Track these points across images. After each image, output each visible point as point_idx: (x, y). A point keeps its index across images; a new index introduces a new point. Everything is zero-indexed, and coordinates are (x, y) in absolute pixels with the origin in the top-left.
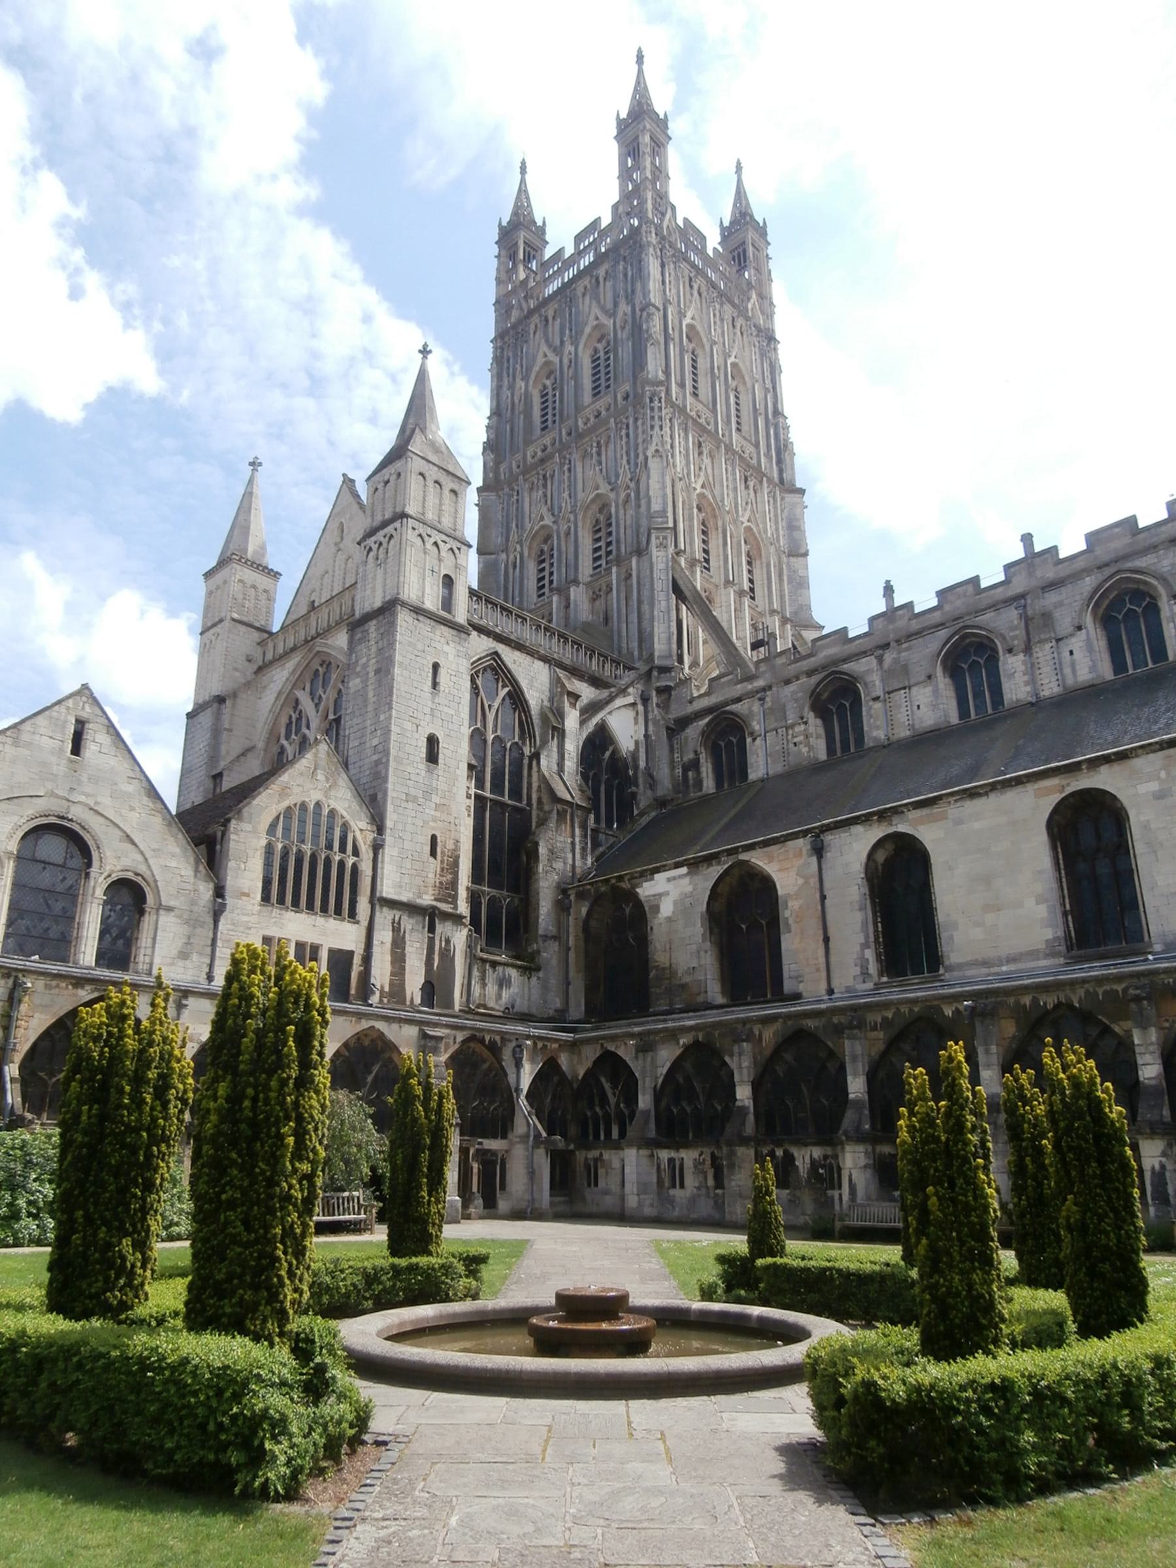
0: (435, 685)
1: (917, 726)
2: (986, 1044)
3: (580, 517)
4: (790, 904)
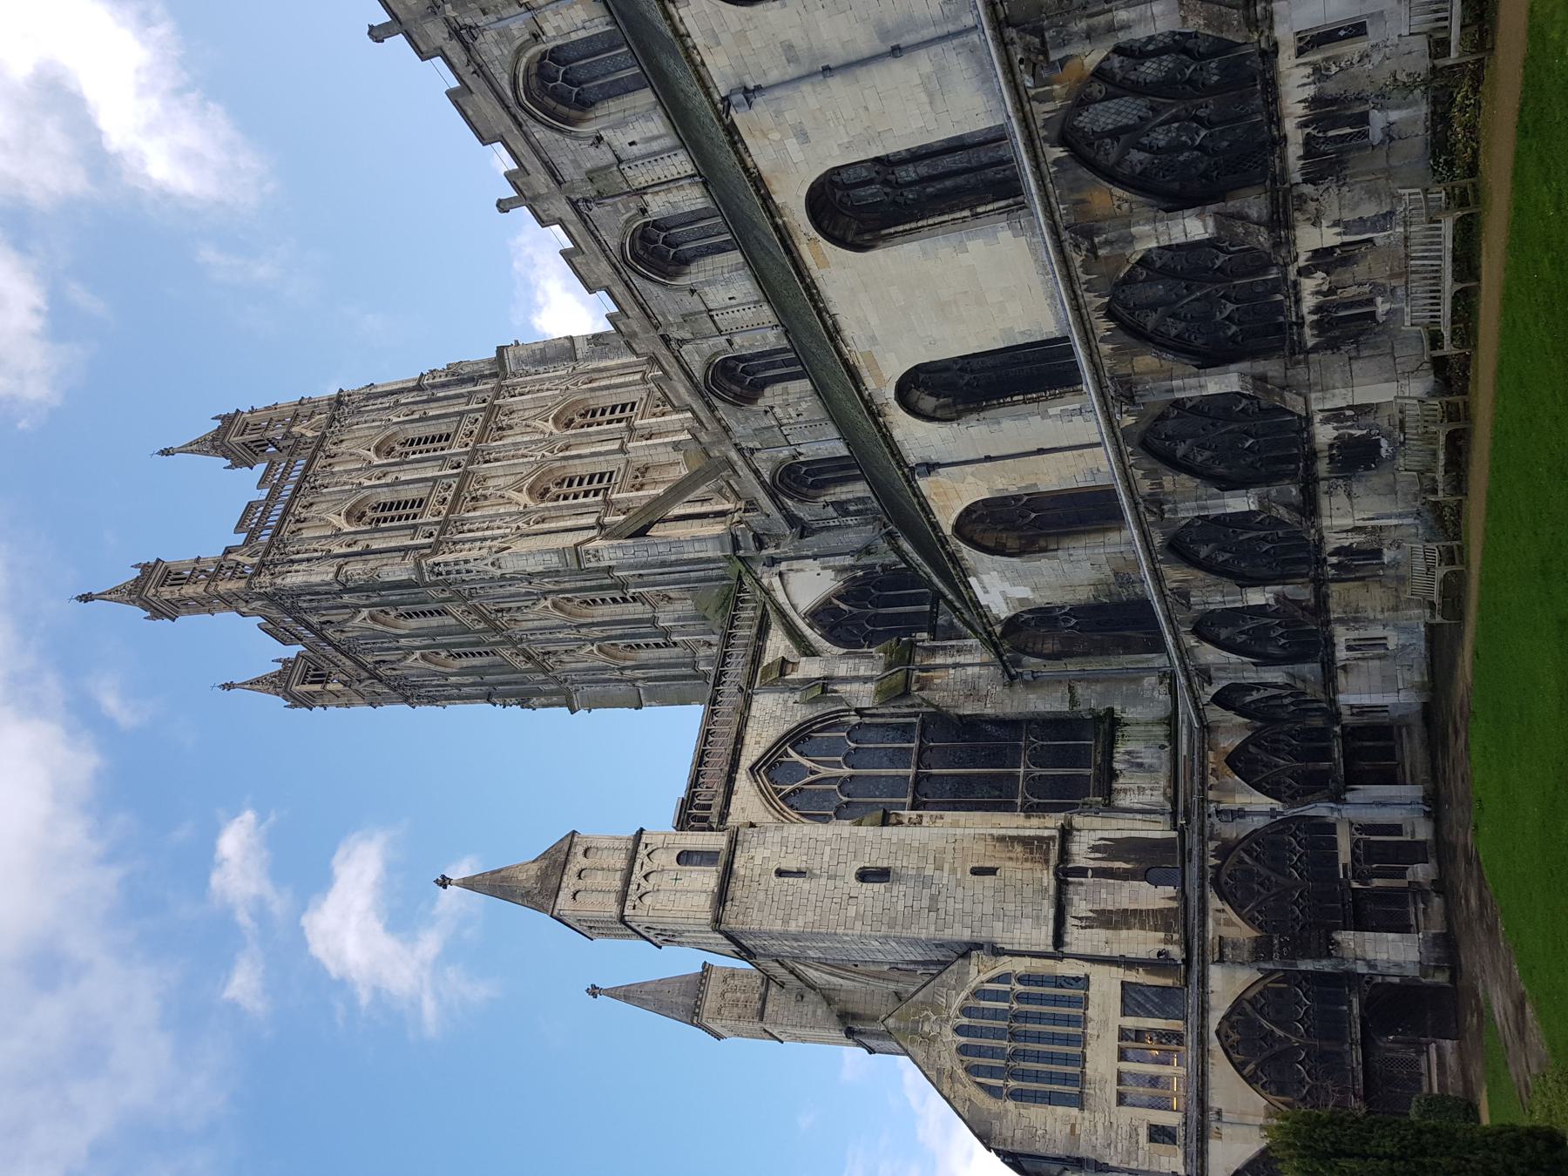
0: (800, 873)
1: (756, 298)
2: (1172, 391)
3: (582, 621)
4: (1001, 487)
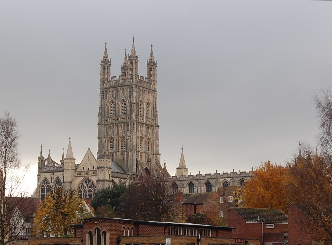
3: (119, 139)
